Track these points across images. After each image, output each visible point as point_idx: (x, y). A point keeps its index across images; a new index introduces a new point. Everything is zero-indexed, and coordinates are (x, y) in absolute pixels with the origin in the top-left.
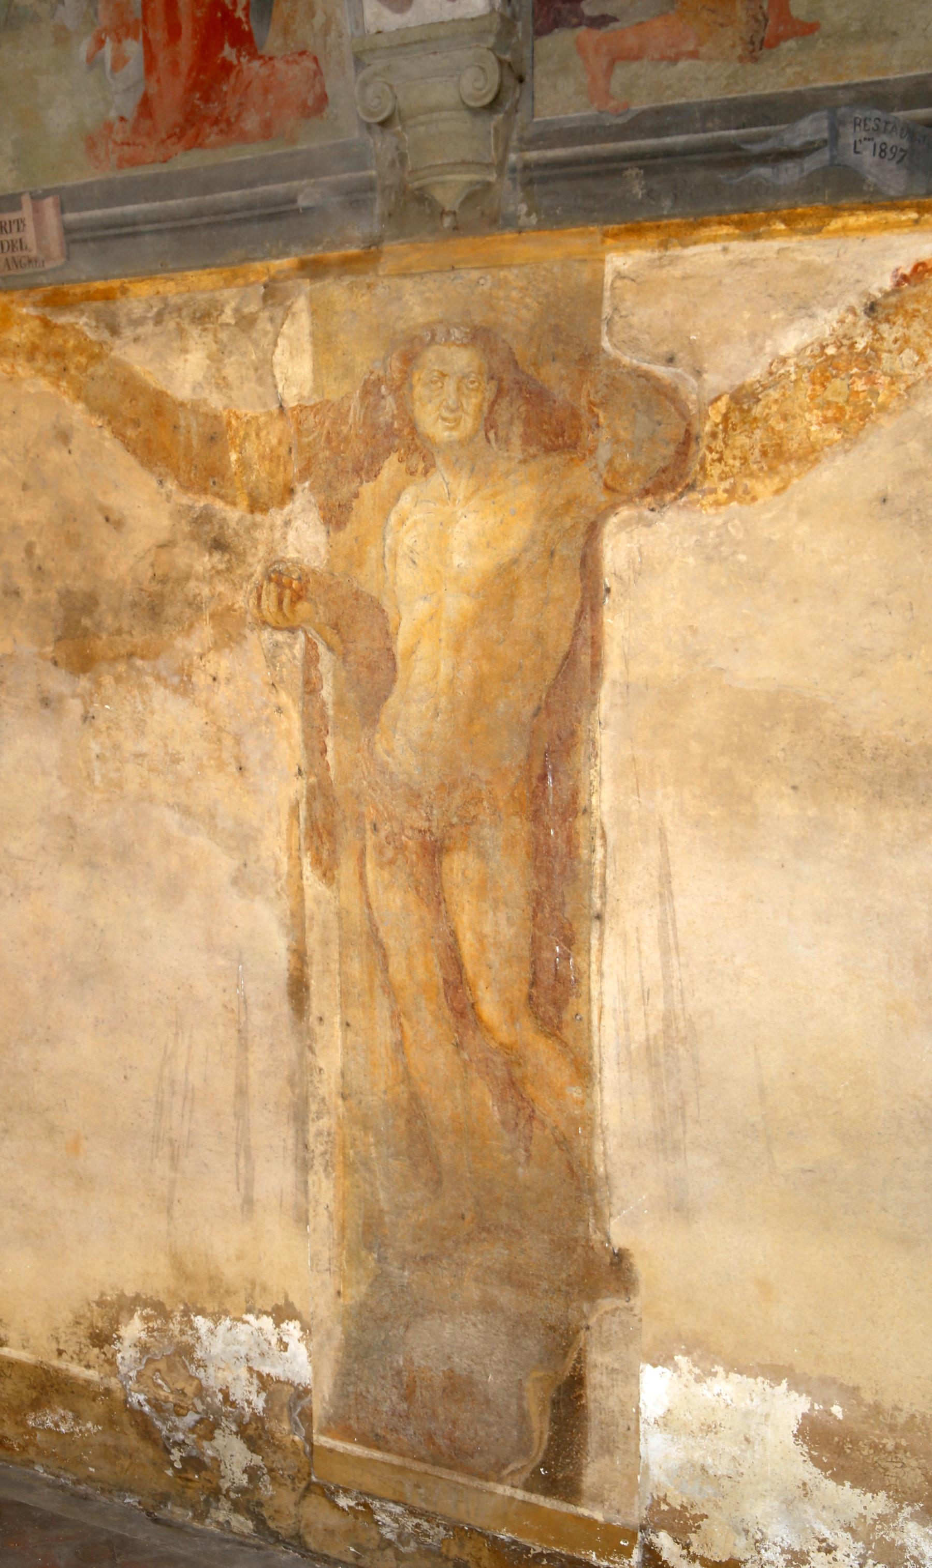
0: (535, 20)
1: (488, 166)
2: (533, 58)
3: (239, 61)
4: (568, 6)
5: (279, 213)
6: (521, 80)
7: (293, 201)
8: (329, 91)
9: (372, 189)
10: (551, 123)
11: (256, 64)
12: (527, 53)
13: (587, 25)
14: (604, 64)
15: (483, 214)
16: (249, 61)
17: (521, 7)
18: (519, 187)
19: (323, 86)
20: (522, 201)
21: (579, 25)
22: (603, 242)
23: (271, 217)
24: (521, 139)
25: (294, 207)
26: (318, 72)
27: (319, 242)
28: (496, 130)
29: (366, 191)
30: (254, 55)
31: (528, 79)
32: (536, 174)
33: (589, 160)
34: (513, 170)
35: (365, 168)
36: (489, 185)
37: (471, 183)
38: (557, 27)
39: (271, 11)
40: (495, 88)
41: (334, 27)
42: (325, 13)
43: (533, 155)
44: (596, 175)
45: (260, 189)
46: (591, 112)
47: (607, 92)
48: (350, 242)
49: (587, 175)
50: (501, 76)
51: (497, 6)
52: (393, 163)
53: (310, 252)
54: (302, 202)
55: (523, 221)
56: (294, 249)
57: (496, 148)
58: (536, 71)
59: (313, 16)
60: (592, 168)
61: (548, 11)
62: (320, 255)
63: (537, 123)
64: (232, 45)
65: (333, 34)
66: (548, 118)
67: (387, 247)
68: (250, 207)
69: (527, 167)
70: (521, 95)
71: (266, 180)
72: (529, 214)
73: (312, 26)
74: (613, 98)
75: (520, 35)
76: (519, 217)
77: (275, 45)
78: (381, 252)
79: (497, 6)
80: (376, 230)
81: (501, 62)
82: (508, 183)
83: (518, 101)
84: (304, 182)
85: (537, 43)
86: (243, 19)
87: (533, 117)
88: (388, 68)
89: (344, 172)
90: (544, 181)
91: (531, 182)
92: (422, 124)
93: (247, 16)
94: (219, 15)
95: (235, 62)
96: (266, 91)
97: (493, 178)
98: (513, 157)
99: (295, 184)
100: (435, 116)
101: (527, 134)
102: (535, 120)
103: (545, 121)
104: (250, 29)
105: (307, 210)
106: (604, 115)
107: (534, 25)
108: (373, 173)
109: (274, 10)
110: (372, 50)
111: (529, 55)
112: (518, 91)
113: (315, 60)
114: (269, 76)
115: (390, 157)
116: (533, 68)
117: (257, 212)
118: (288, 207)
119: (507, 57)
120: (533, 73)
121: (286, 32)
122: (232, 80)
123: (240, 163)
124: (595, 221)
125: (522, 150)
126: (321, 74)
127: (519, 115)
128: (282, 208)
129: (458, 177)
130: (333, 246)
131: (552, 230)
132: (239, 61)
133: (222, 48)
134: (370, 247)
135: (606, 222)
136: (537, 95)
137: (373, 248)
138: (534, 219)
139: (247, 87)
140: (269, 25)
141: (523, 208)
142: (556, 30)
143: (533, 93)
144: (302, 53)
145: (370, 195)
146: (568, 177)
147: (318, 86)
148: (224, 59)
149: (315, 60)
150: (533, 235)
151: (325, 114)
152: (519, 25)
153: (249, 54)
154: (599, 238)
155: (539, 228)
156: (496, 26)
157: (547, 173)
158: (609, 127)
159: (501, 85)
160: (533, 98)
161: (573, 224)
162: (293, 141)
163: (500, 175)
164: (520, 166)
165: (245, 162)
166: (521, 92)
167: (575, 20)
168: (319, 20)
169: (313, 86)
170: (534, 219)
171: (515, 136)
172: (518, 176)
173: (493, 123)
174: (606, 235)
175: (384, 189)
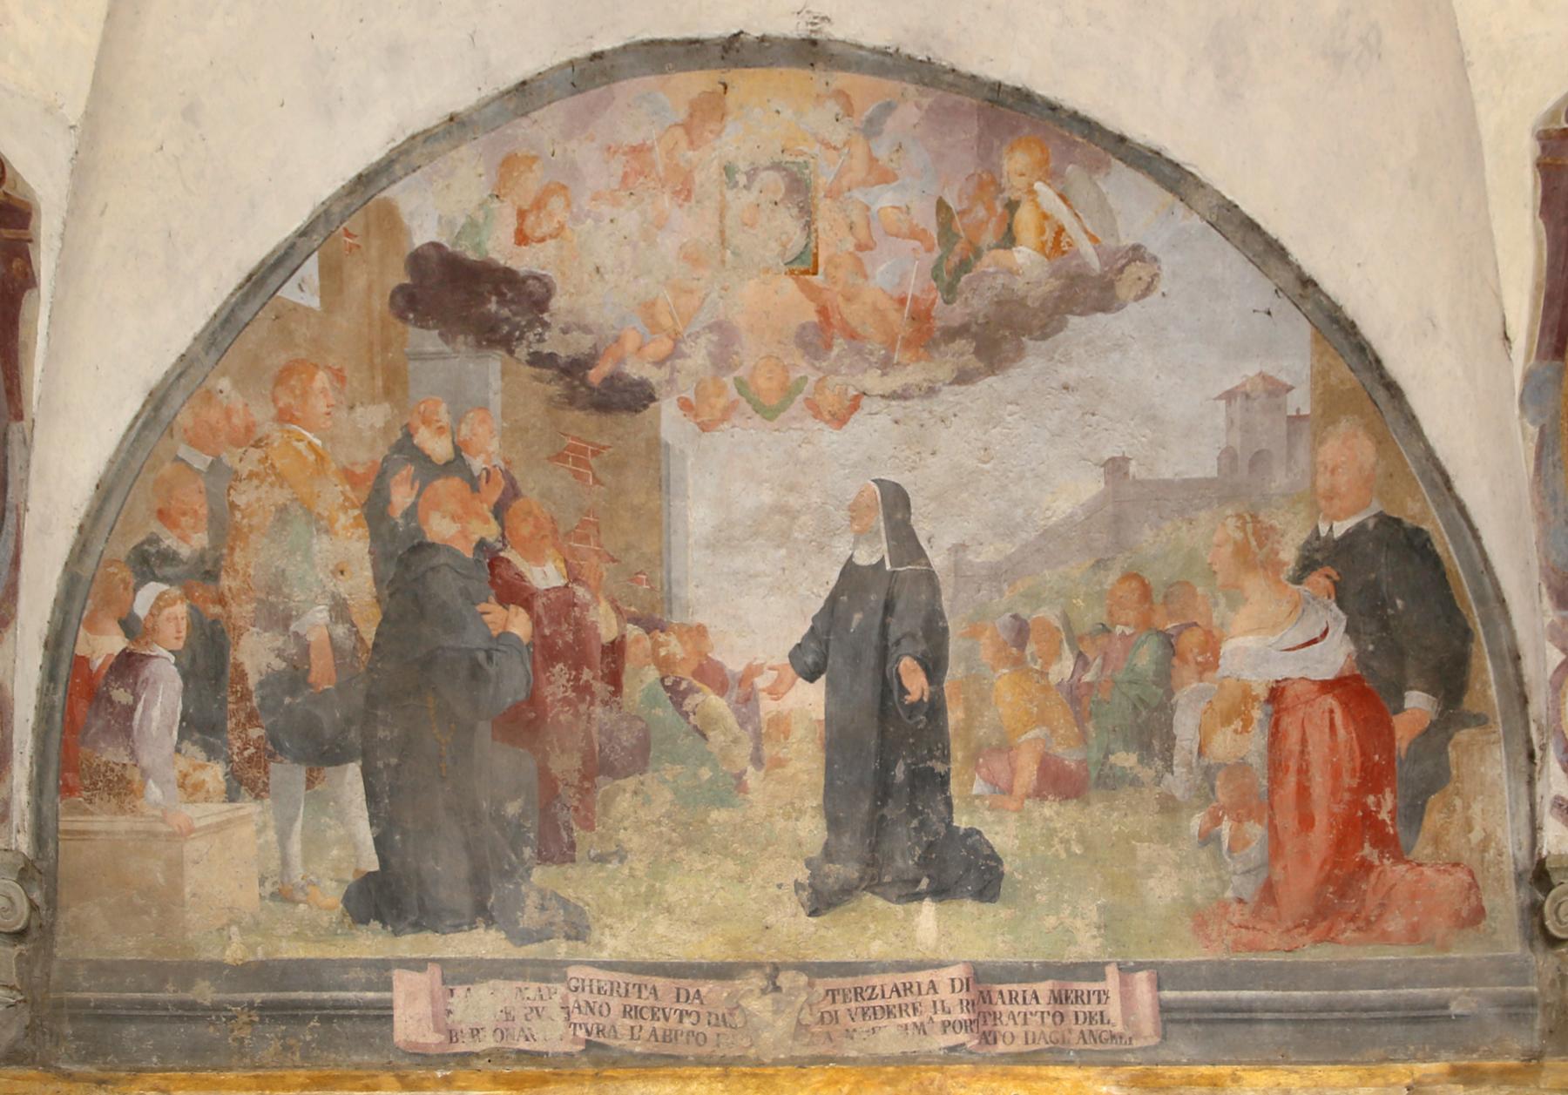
3: (1381, 862)
5: (1426, 1017)
7: (1445, 1007)
8: (1486, 904)
9: (1533, 1005)
11: (1402, 868)
16: (1394, 864)
19: (1479, 900)
23: (1416, 1020)
25: (1445, 1013)
26: (1474, 885)
27: (1474, 1051)
29: (1527, 1006)
30: (1399, 857)
35: (1526, 984)
39: (1421, 819)
41: (1493, 844)
42: (1484, 830)
45: (1404, 991)
48: (1509, 1053)
53: (1464, 1059)
54: (1455, 1009)
56: (1444, 1054)
59: (1470, 832)
62: (1475, 1063)
64: (1374, 845)
65: (1492, 852)
68: (1392, 1007)
71: (1410, 982)
73: (1469, 841)
77: (1425, 852)
78: (1542, 1066)
80: (1537, 1044)
84: (1458, 990)
86: (1389, 822)
89: (1502, 985)
93: (1393, 819)
94: (1360, 814)
95: (1377, 863)
96: (1414, 896)
99: (1448, 990)
104: (1396, 834)
105: (1460, 1018)
108: (1535, 989)
109: (1426, 818)
113: (1471, 873)
114: (1417, 882)
115: (1550, 976)
117: (1400, 1014)
118: (1438, 1012)
121: (1436, 840)
122: (1373, 877)
123: (1381, 962)
126: (1478, 887)
128: (1431, 1013)
130: (1490, 1055)
132: (1381, 862)
133: (1362, 847)
134: (1530, 1060)
137: (1534, 1062)
139: (1391, 889)
140: (1418, 832)
144: (1456, 865)
145: (1531, 1010)
147: (1473, 899)
149: (1471, 873)
151: (1481, 926)
153: (1394, 857)
162: (1445, 948)
165: (1388, 962)
168: (1476, 836)
169: (1468, 898)
175: (1546, 1006)
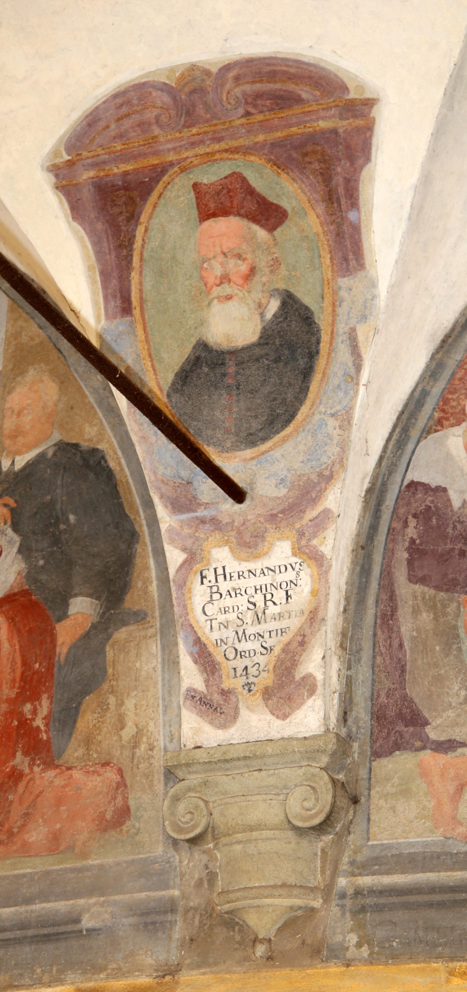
0: (373, 741)
1: (313, 890)
2: (370, 779)
3: (31, 770)
4: (411, 729)
5: (57, 934)
6: (355, 801)
7: (77, 921)
8: (131, 803)
9: (173, 910)
10: (390, 847)
11: (51, 774)
12: (363, 773)
13: (431, 749)
14: (452, 789)
15: (303, 943)
16: (43, 771)
17: (358, 728)
18: (348, 915)
19: (125, 799)
20: (352, 930)
21: (423, 748)
22: (448, 981)
23: (47, 938)
24: (352, 863)
25: (76, 927)
26: (122, 784)
27: (102, 969)
28: (323, 850)
29: (165, 912)
30: (49, 764)
31: (363, 800)
32: (369, 901)
33: (433, 889)
34: (343, 896)
35: (167, 887)
36: (313, 910)
37: (291, 908)
38: (399, 749)
39: (75, 722)
40: (327, 809)
41: (145, 739)
42: (137, 726)
43: (366, 881)
44: (441, 905)
45: (37, 907)
46: (437, 837)
47: (454, 818)
48: (141, 970)
49: (431, 905)
50: (334, 797)
51: (332, 726)
52: (199, 884)
53: (90, 980)
54: (87, 923)
55: (352, 953)
56: (70, 976)
57: (323, 872)
58: (373, 792)
59: (122, 728)
60: (437, 898)
61: (389, 734)
62: (102, 984)
63: (372, 845)
64: (26, 753)
65: (143, 747)
66: (386, 842)
67: (185, 977)
68: (23, 926)
69: (358, 893)
70: (354, 816)
71: (44, 897)
72: (359, 945)
73: (120, 738)
74: (461, 824)
75: (356, 755)
76: (347, 949)
77: (76, 755)
78: (177, 983)
79: (332, 726)
80: (174, 958)
81: (334, 781)
82: (335, 910)
83: (351, 822)
84: (92, 900)
85: (374, 764)
86: (43, 728)
87: (368, 839)
88: (205, 783)
89: (141, 890)
90: (379, 909)
91: (363, 909)
92: (239, 842)
93: (47, 725)
94: (16, 723)
95: (27, 771)
96: (59, 801)
97: (317, 903)
98: (342, 882)
99: (82, 902)
100: (255, 834)
101: (359, 858)
102: (370, 843)
103: (382, 845)
104: (49, 738)
105: (91, 931)
106: (450, 841)
107: (371, 747)
108: (176, 893)
109: (79, 720)
110: (187, 765)
111: (366, 776)
112: (352, 812)
113: (120, 771)
114: (64, 787)
115: (197, 876)
116: (370, 789)
117: (30, 933)
118: (69, 928)
119: (341, 777)
120: (369, 795)
121: (88, 741)
122: (21, 787)
123: (17, 877)
124: (439, 957)
125: (353, 875)
126: (126, 786)
127: (351, 837)
128: (62, 929)
129: (276, 901)
130: (119, 973)
131: (386, 964)
132: (31, 770)
133: (14, 756)
134: (164, 977)
135: (452, 959)
136: (372, 818)
137: (168, 978)
138: (365, 951)
139: (38, 796)
140: (71, 735)
141: (353, 938)
142: (397, 752)
143: (369, 815)
144: (106, 764)
145: (169, 917)
146: (407, 906)
147: (120, 798)
148: (14, 769)
149: (120, 771)
150: (364, 969)
151: (124, 828)
152: (356, 745)
153: (44, 763)
154: (444, 976)
155: (371, 961)
156: (332, 746)
157: (382, 900)
158: (456, 854)
159: (333, 805)
160: (369, 820)
161: (413, 959)
162: (84, 855)
163: (326, 900)
164: (351, 891)
165: (24, 876)
166: (355, 813)
167: (418, 744)
168: (128, 732)
169: (115, 798)
170: (365, 951)
171: (345, 859)
172: (348, 902)
173: (320, 845)
174: (451, 973)
175: (187, 911)
